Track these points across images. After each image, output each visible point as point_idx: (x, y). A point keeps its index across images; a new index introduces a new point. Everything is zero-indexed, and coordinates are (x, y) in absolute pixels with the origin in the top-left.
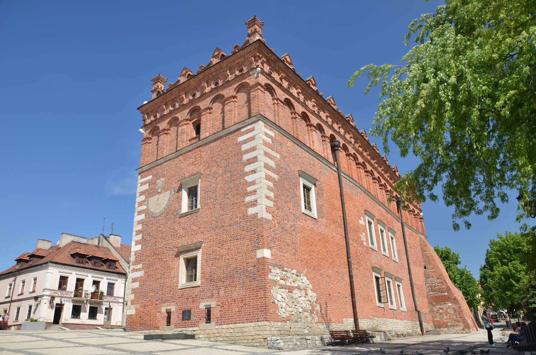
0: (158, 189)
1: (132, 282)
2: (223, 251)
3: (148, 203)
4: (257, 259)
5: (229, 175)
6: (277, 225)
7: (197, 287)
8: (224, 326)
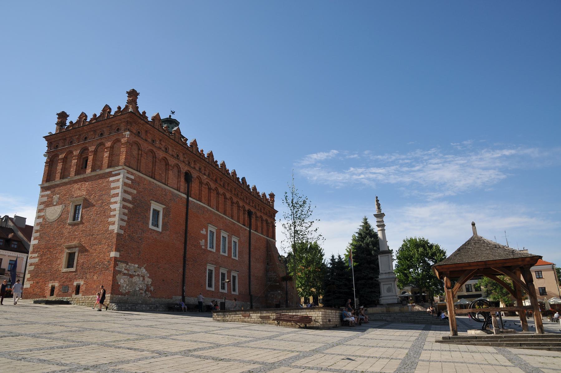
3: (45, 211)
4: (110, 257)
6: (127, 237)
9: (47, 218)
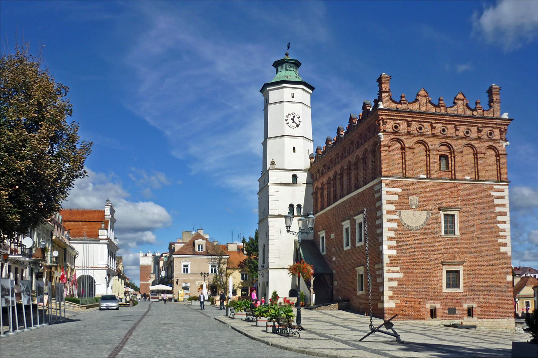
0: (412, 205)
1: (388, 281)
2: (482, 271)
3: (400, 215)
4: (507, 281)
5: (484, 218)
7: (460, 292)
8: (485, 320)
9: (405, 224)
